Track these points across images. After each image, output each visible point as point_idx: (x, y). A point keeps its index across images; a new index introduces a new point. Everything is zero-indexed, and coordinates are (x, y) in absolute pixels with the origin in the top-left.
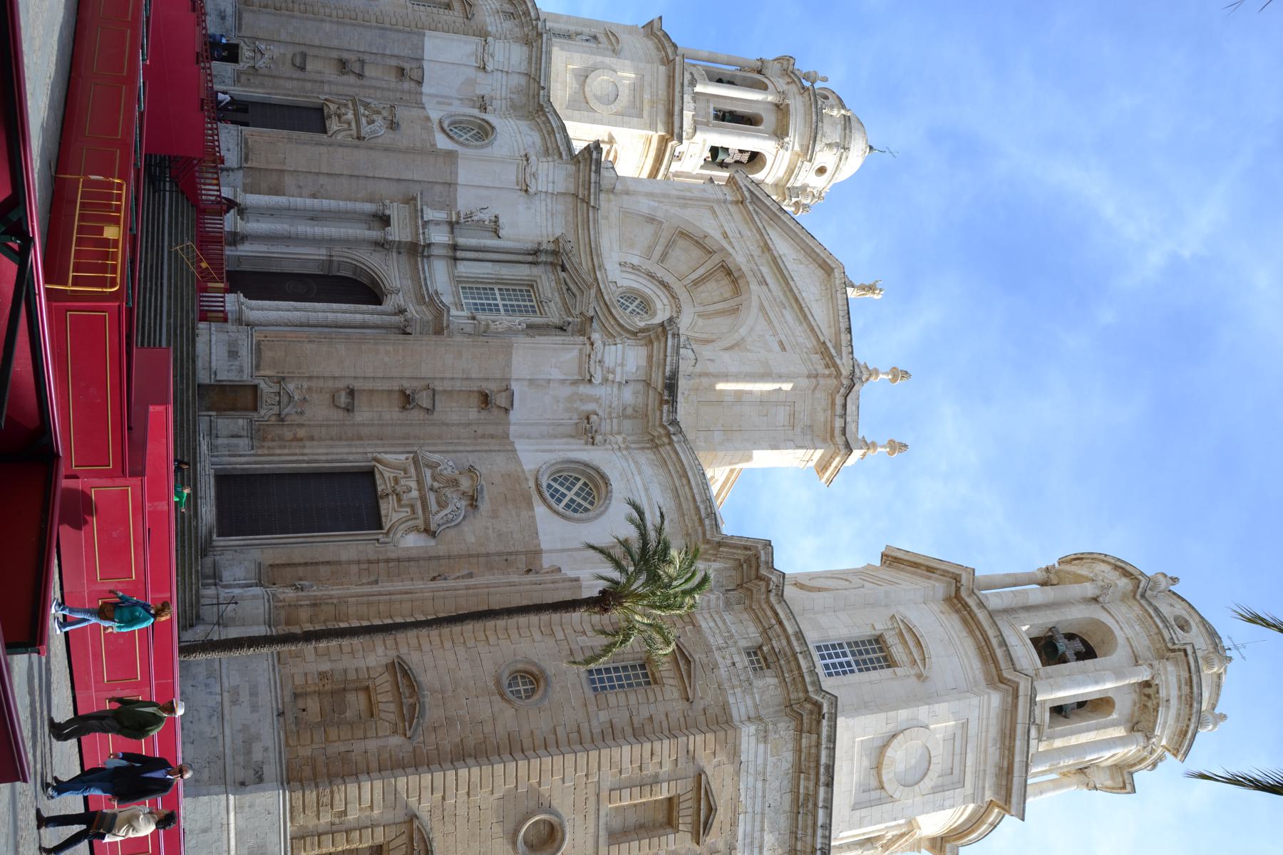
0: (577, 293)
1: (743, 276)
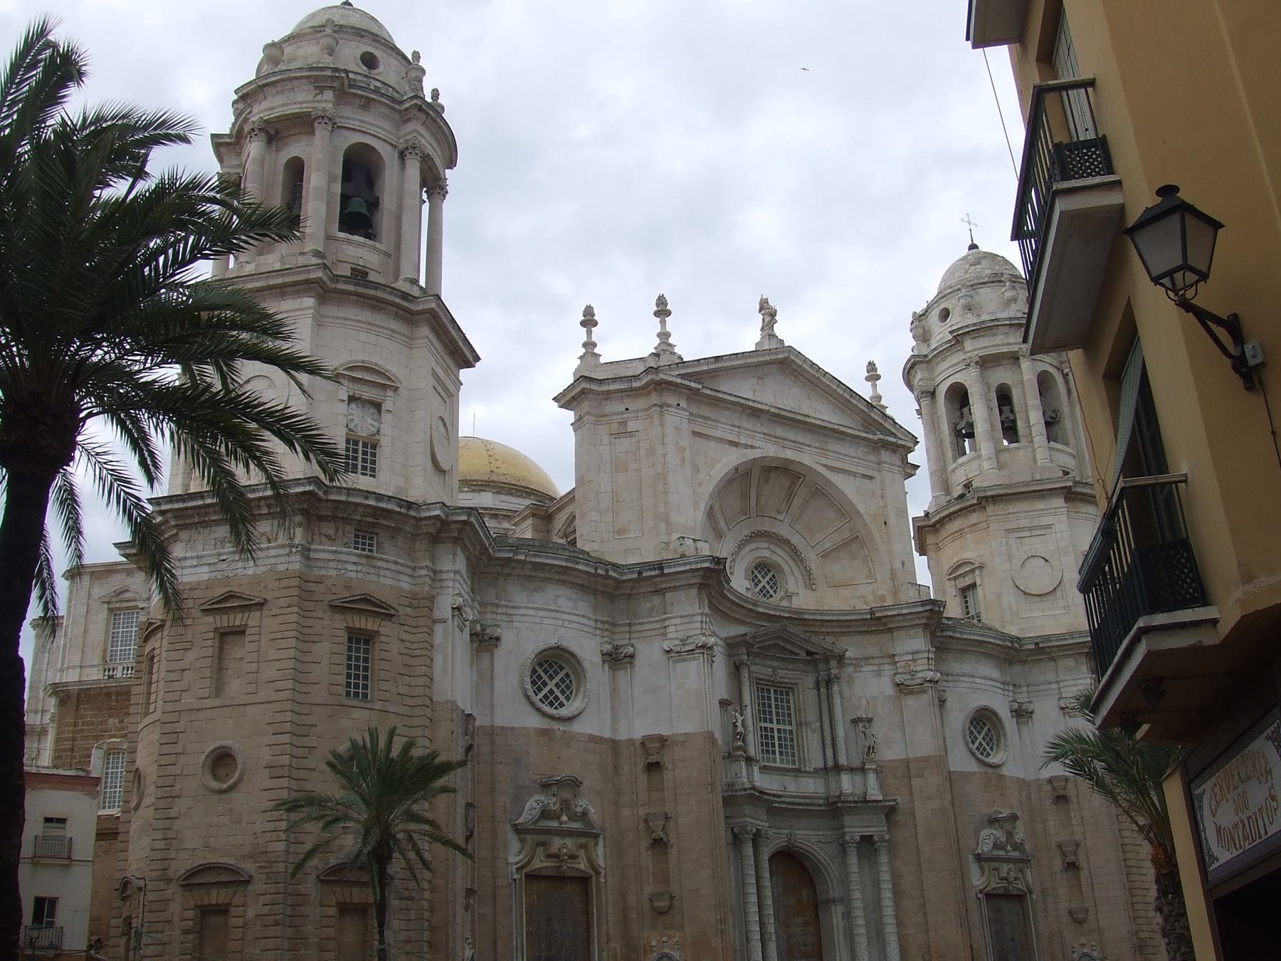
0: (776, 641)
1: (792, 462)
